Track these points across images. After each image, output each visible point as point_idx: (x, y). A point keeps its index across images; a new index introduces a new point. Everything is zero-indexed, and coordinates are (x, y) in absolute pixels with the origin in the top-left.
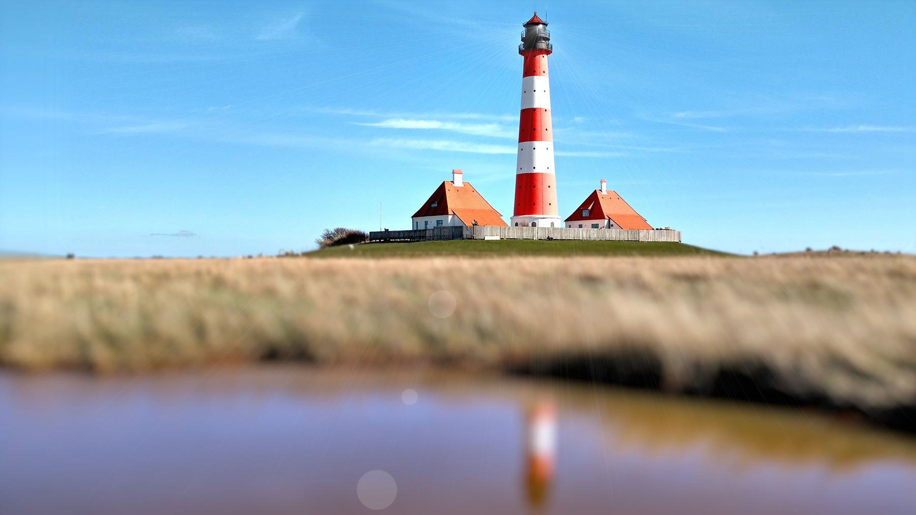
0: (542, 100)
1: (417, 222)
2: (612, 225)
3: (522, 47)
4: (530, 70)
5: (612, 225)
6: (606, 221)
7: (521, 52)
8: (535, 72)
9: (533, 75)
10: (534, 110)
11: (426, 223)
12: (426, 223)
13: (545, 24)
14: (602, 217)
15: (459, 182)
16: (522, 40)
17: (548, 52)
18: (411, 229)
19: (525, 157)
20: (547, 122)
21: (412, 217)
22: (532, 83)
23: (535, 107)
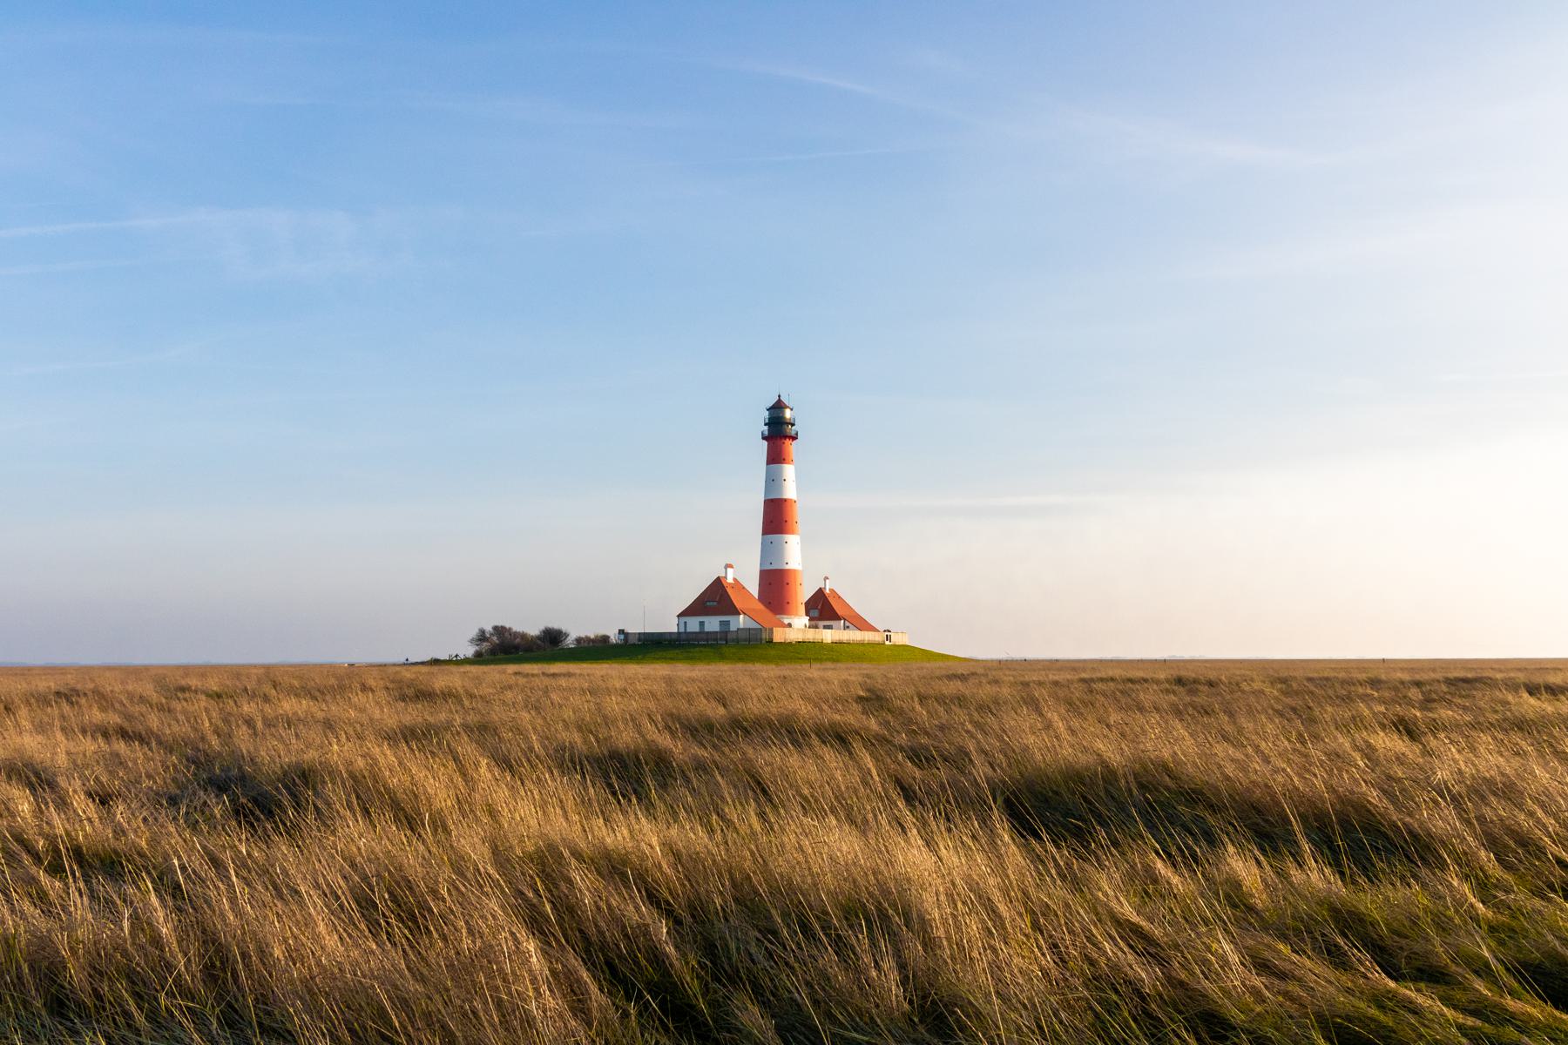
0: (790, 491)
1: (685, 623)
2: (848, 627)
3: (766, 433)
4: (776, 457)
5: (848, 627)
6: (842, 621)
7: (764, 438)
8: (784, 459)
9: (782, 463)
10: (785, 500)
11: (702, 624)
12: (702, 624)
13: (792, 409)
14: (837, 617)
15: (730, 580)
16: (766, 424)
17: (794, 438)
18: (676, 631)
19: (768, 551)
20: (800, 515)
21: (678, 616)
22: (780, 473)
23: (785, 497)
